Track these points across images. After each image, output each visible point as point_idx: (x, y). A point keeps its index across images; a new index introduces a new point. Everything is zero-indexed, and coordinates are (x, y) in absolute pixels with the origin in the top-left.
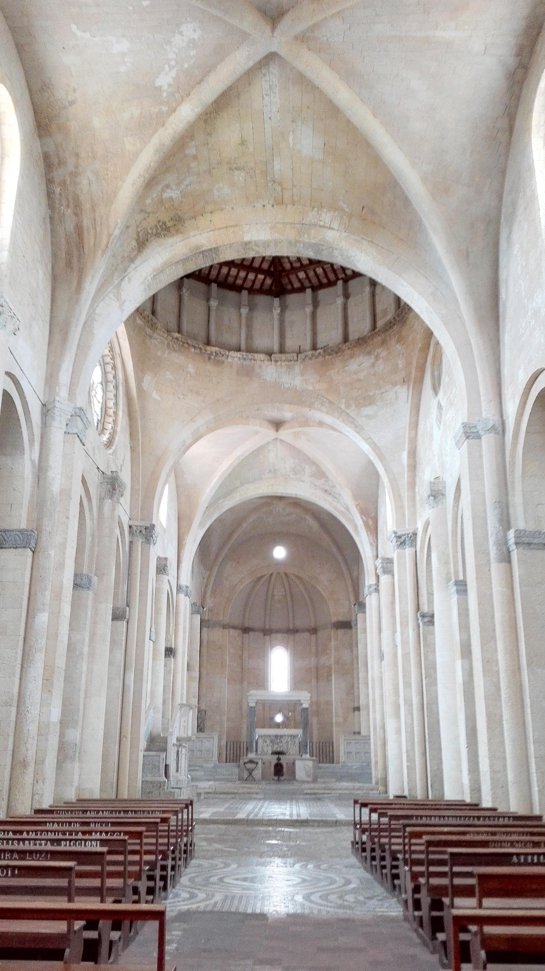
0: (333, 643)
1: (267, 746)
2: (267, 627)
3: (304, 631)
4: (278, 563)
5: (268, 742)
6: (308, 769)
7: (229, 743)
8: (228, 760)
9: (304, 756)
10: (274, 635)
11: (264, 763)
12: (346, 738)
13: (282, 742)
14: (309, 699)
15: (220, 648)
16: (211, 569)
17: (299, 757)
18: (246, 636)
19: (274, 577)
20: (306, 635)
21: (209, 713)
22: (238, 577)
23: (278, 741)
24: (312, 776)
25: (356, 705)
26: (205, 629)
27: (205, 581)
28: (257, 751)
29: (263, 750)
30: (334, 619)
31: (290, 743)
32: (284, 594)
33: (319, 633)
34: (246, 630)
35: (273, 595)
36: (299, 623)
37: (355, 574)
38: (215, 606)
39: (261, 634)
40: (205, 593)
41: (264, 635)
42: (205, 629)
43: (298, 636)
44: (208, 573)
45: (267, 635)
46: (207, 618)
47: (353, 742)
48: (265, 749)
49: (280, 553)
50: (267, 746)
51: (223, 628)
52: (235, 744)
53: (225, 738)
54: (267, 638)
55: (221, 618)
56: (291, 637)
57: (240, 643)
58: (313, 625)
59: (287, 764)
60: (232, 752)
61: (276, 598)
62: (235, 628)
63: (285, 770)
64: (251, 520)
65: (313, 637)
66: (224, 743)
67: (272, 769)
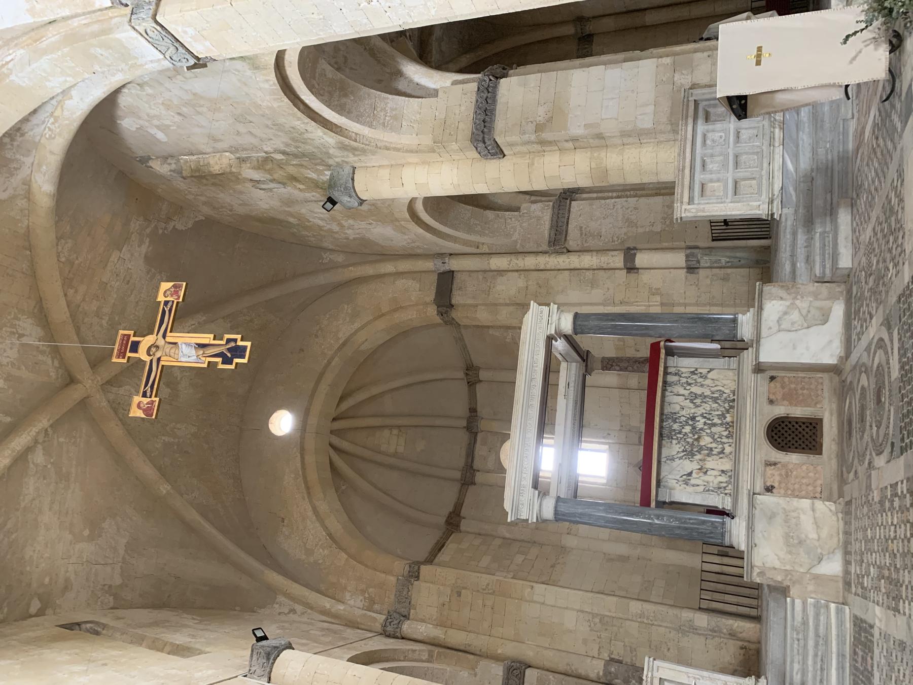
0: (483, 316)
1: (703, 471)
2: (458, 475)
3: (473, 396)
4: (303, 427)
5: (689, 466)
6: (795, 316)
7: (704, 604)
8: (753, 612)
9: (745, 330)
10: (477, 464)
11: (769, 489)
12: (686, 199)
13: (693, 418)
14: (545, 309)
15: (459, 594)
16: (272, 592)
17: (748, 357)
18: (464, 525)
19: (344, 445)
20: (481, 390)
21: (618, 651)
22: (309, 525)
23: (687, 429)
24: (826, 304)
25: (618, 260)
26: (407, 627)
27: (299, 608)
28: (722, 513)
29: (719, 489)
30: (432, 311)
31: (695, 389)
32: (395, 432)
33: (477, 360)
34: (453, 522)
35: (395, 455)
36: (461, 408)
37: (340, 258)
38: (363, 592)
39: (472, 488)
40: (325, 612)
41: (473, 483)
42: (407, 627)
43: (483, 411)
44: (281, 598)
45: (473, 476)
46: (384, 617)
47: (699, 177)
48: (713, 479)
49: (283, 423)
50: (703, 471)
51: (417, 578)
52: (706, 585)
53: (687, 615)
54: (479, 478)
55: (393, 579)
56: (483, 425)
57: (477, 542)
58: (461, 375)
59: (771, 402)
60: (728, 598)
61: (401, 449)
62: (439, 547)
63: (798, 412)
64: (148, 471)
65: (483, 375)
66: (702, 620)
67: (794, 458)
